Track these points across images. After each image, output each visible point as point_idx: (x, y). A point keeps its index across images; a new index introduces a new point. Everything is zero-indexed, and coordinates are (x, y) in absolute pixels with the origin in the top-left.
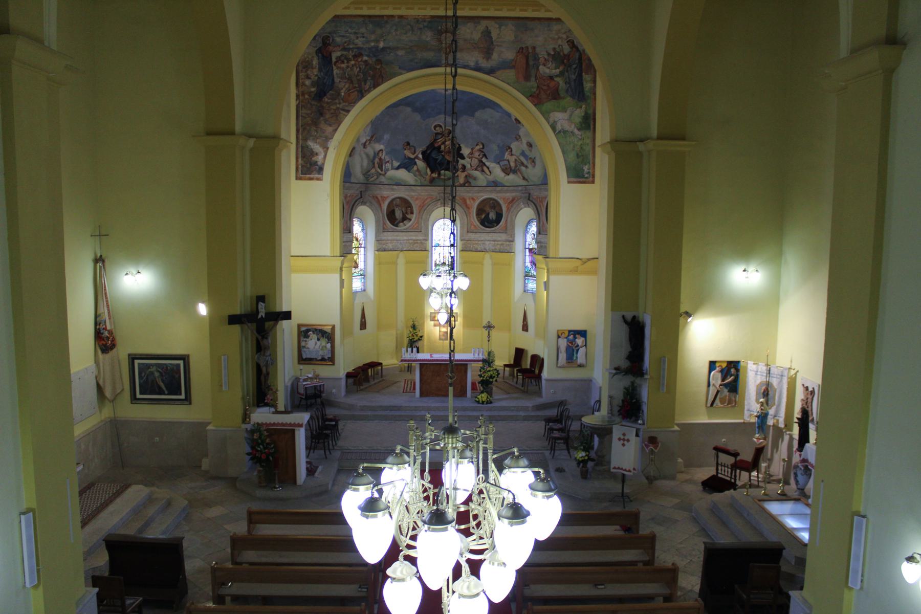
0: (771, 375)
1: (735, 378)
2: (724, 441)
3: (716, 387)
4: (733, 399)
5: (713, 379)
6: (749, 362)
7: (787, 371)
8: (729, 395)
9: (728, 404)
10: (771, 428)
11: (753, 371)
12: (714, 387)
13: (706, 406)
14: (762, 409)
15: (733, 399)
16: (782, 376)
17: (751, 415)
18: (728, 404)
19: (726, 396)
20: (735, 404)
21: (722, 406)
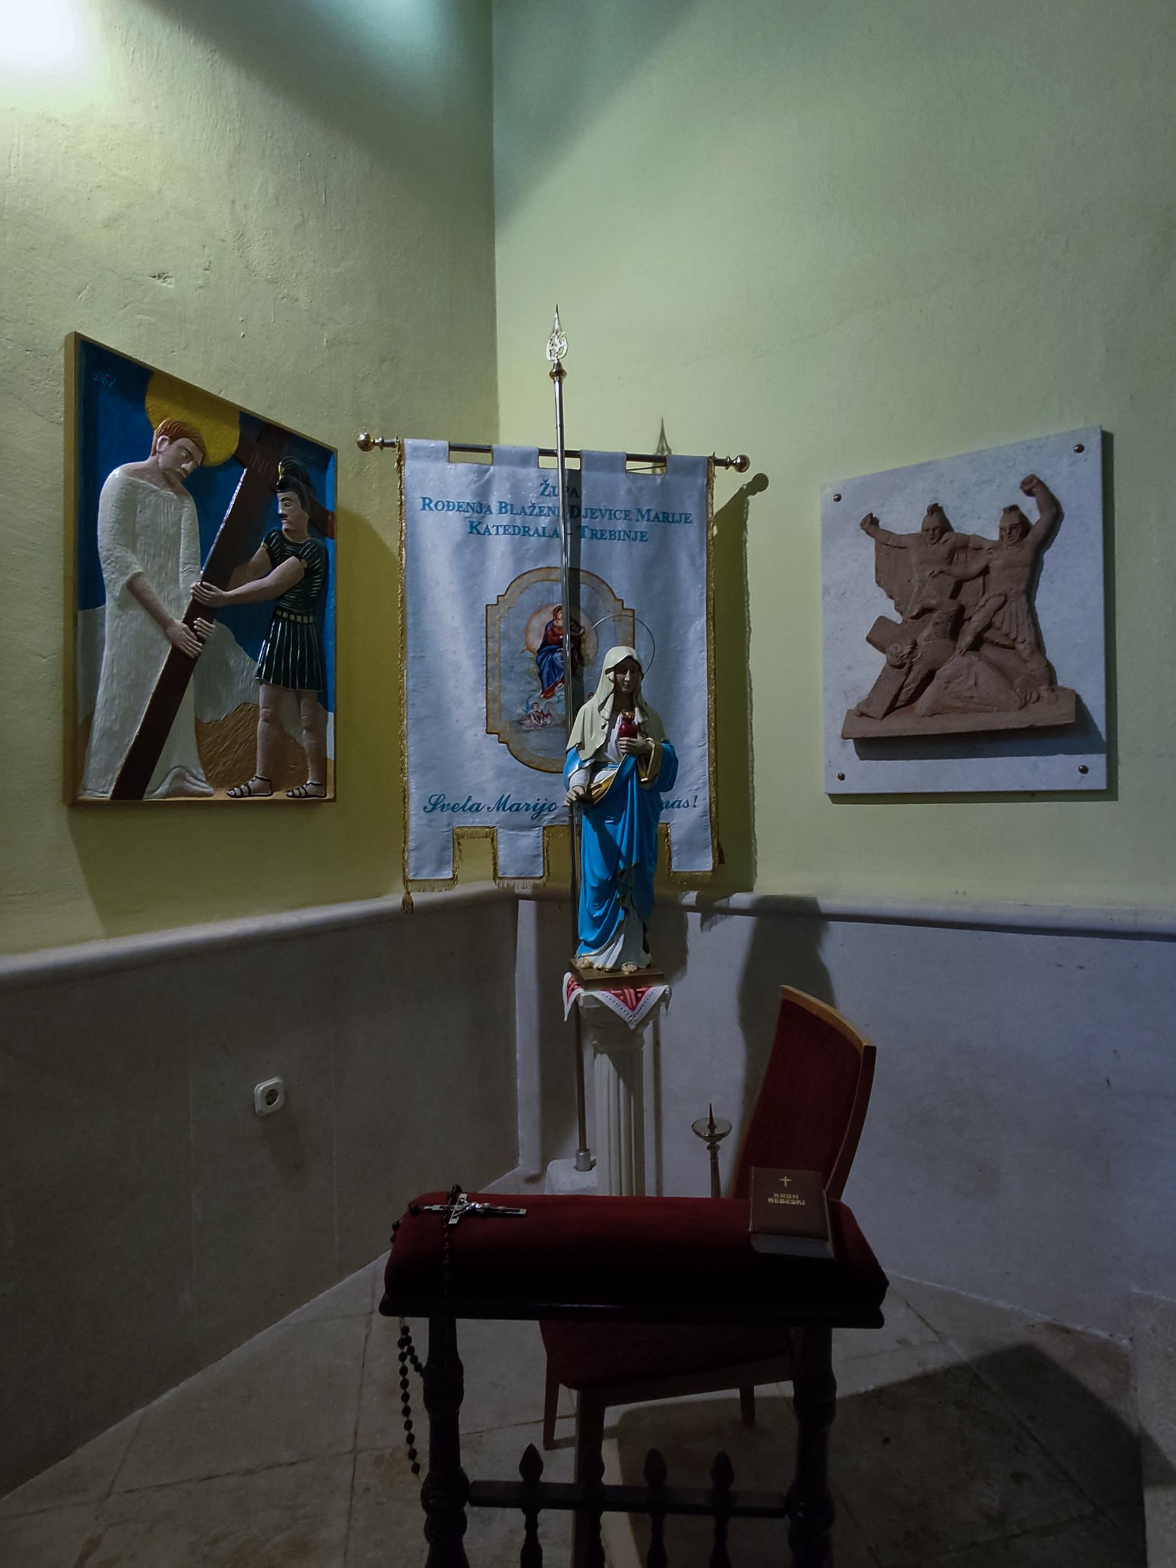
0: (584, 522)
1: (309, 573)
2: (271, 1095)
3: (163, 623)
4: (305, 740)
5: (127, 532)
6: (409, 442)
7: (701, 481)
8: (273, 703)
9: (271, 784)
10: (527, 911)
11: (448, 506)
12: (138, 614)
13: (75, 804)
14: (629, 730)
15: (305, 740)
16: (665, 518)
17: (457, 839)
18: (271, 784)
19: (248, 712)
20: (322, 784)
21: (221, 795)
